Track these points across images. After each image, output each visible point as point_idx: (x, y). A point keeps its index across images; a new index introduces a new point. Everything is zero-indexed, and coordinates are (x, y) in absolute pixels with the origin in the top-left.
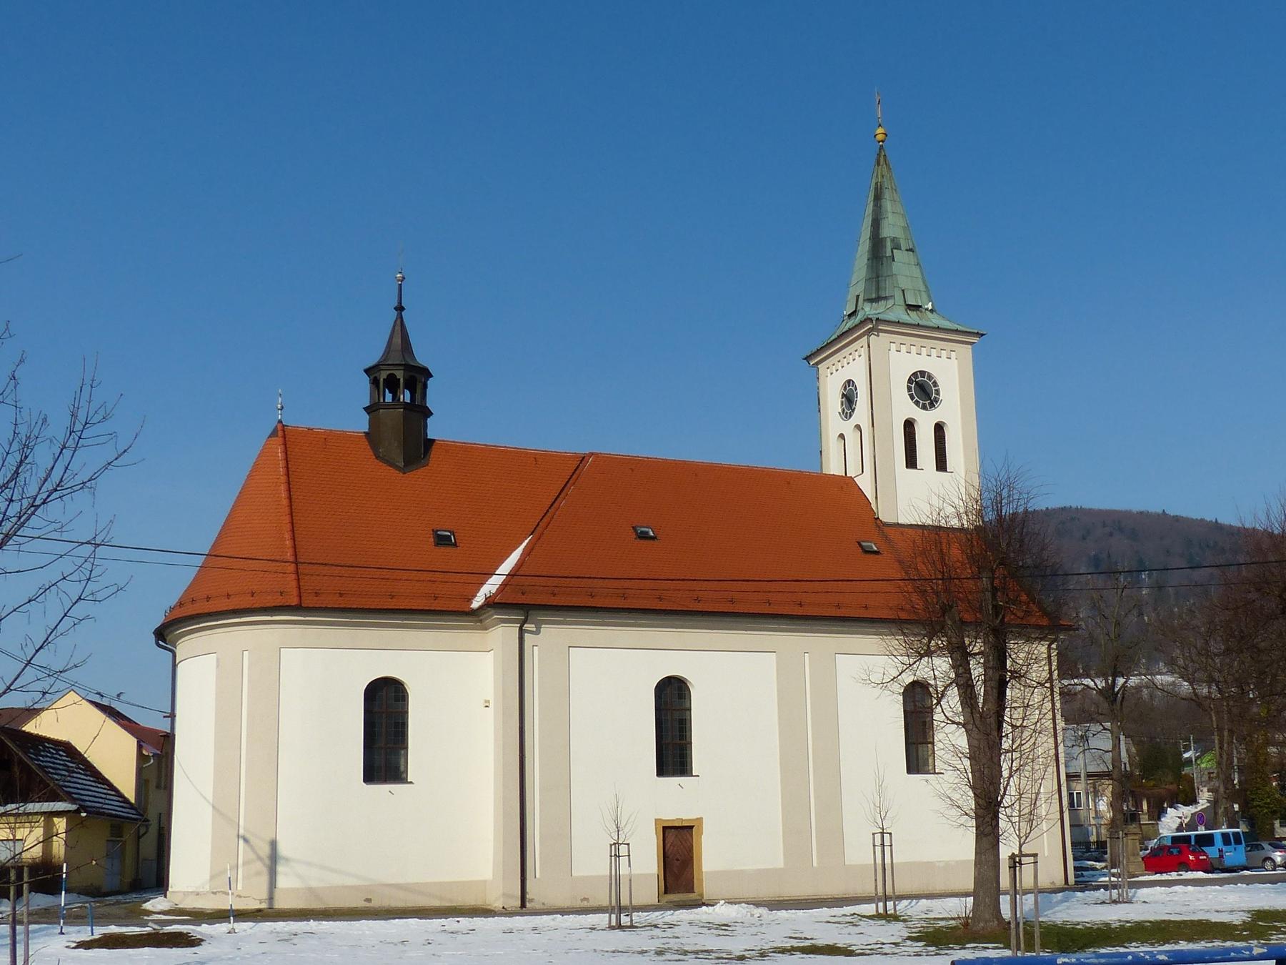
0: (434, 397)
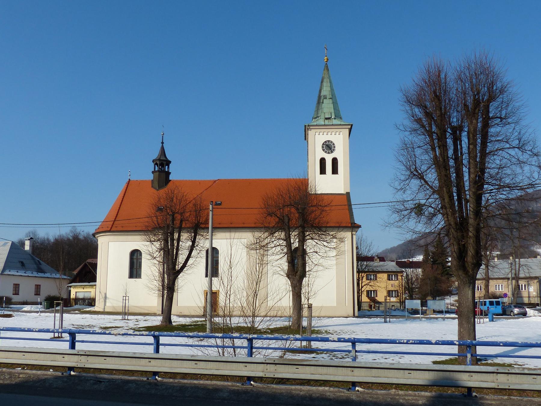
0: (172, 168)
